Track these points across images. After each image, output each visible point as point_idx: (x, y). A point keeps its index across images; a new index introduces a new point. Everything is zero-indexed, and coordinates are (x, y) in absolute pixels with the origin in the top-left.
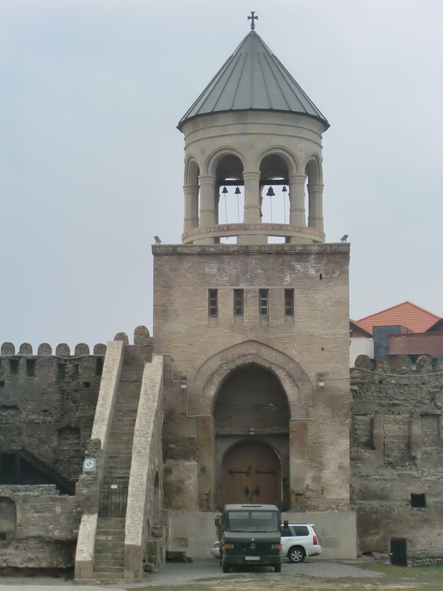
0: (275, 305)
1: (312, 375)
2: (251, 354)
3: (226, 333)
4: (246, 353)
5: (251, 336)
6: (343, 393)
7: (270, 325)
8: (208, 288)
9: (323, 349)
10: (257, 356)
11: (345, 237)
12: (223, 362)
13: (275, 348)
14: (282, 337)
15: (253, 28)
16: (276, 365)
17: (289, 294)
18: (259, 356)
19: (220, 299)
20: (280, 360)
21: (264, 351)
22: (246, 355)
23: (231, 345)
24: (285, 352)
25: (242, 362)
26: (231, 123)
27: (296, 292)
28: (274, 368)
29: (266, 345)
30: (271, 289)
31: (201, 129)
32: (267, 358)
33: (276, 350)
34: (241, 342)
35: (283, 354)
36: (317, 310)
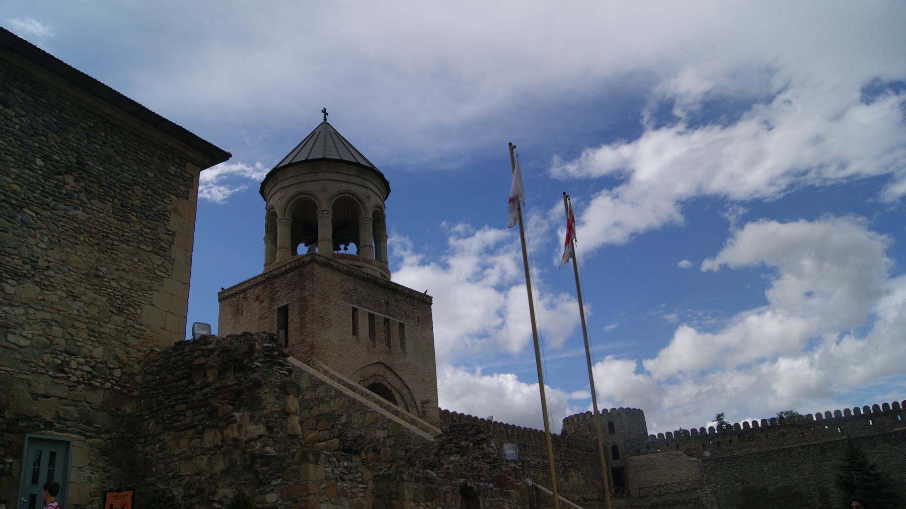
0: (394, 334)
1: (418, 402)
2: (380, 376)
3: (365, 351)
4: (377, 374)
5: (382, 358)
6: (436, 421)
7: (392, 351)
8: (353, 305)
9: (423, 380)
10: (383, 377)
11: (426, 291)
12: (361, 379)
13: (396, 372)
14: (400, 364)
15: (325, 119)
16: (396, 389)
17: (402, 325)
18: (385, 379)
19: (360, 319)
20: (398, 384)
21: (388, 373)
22: (376, 376)
23: (368, 364)
24: (402, 378)
25: (373, 382)
26: (354, 174)
27: (406, 327)
28: (394, 391)
29: (391, 370)
30: (392, 320)
31: (323, 172)
32: (390, 381)
33: (396, 375)
34: (375, 362)
35: (400, 379)
36: (418, 346)
